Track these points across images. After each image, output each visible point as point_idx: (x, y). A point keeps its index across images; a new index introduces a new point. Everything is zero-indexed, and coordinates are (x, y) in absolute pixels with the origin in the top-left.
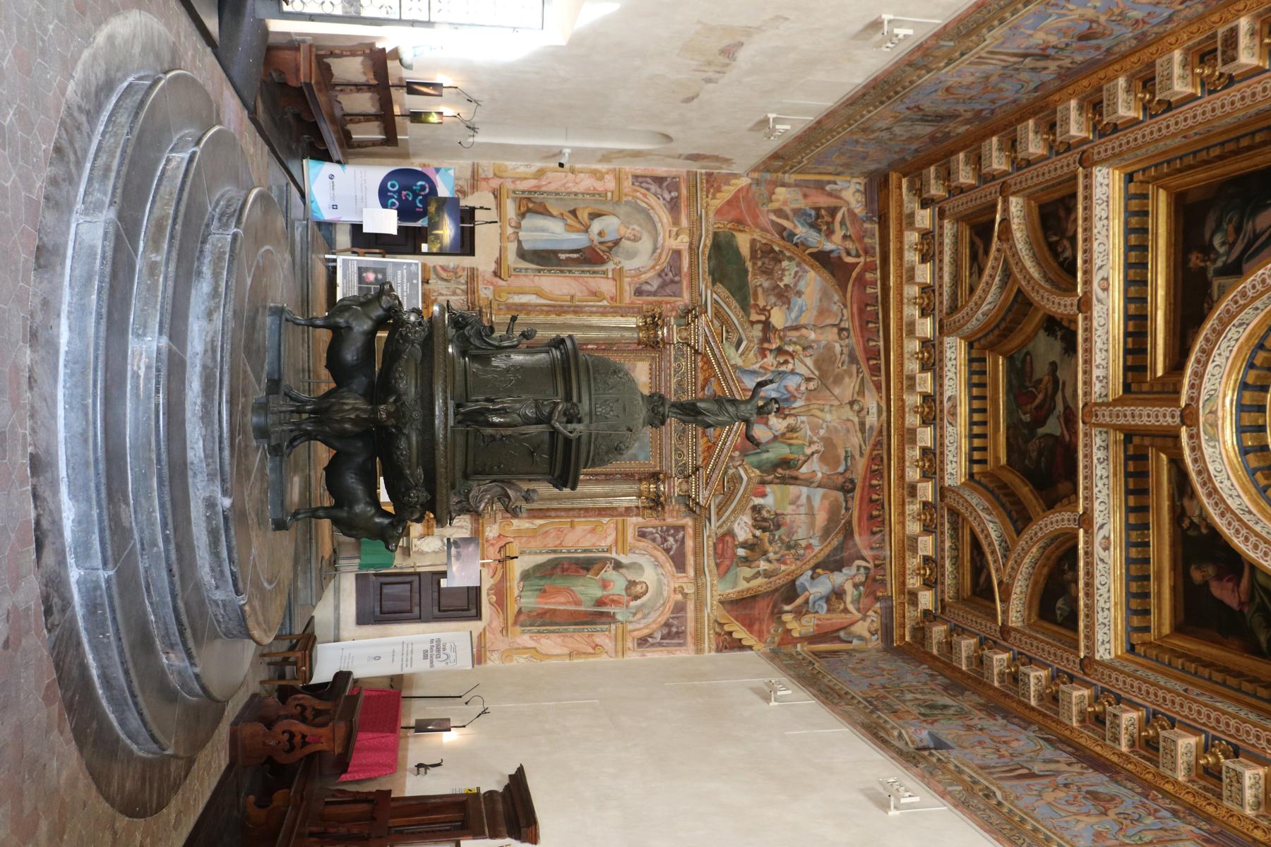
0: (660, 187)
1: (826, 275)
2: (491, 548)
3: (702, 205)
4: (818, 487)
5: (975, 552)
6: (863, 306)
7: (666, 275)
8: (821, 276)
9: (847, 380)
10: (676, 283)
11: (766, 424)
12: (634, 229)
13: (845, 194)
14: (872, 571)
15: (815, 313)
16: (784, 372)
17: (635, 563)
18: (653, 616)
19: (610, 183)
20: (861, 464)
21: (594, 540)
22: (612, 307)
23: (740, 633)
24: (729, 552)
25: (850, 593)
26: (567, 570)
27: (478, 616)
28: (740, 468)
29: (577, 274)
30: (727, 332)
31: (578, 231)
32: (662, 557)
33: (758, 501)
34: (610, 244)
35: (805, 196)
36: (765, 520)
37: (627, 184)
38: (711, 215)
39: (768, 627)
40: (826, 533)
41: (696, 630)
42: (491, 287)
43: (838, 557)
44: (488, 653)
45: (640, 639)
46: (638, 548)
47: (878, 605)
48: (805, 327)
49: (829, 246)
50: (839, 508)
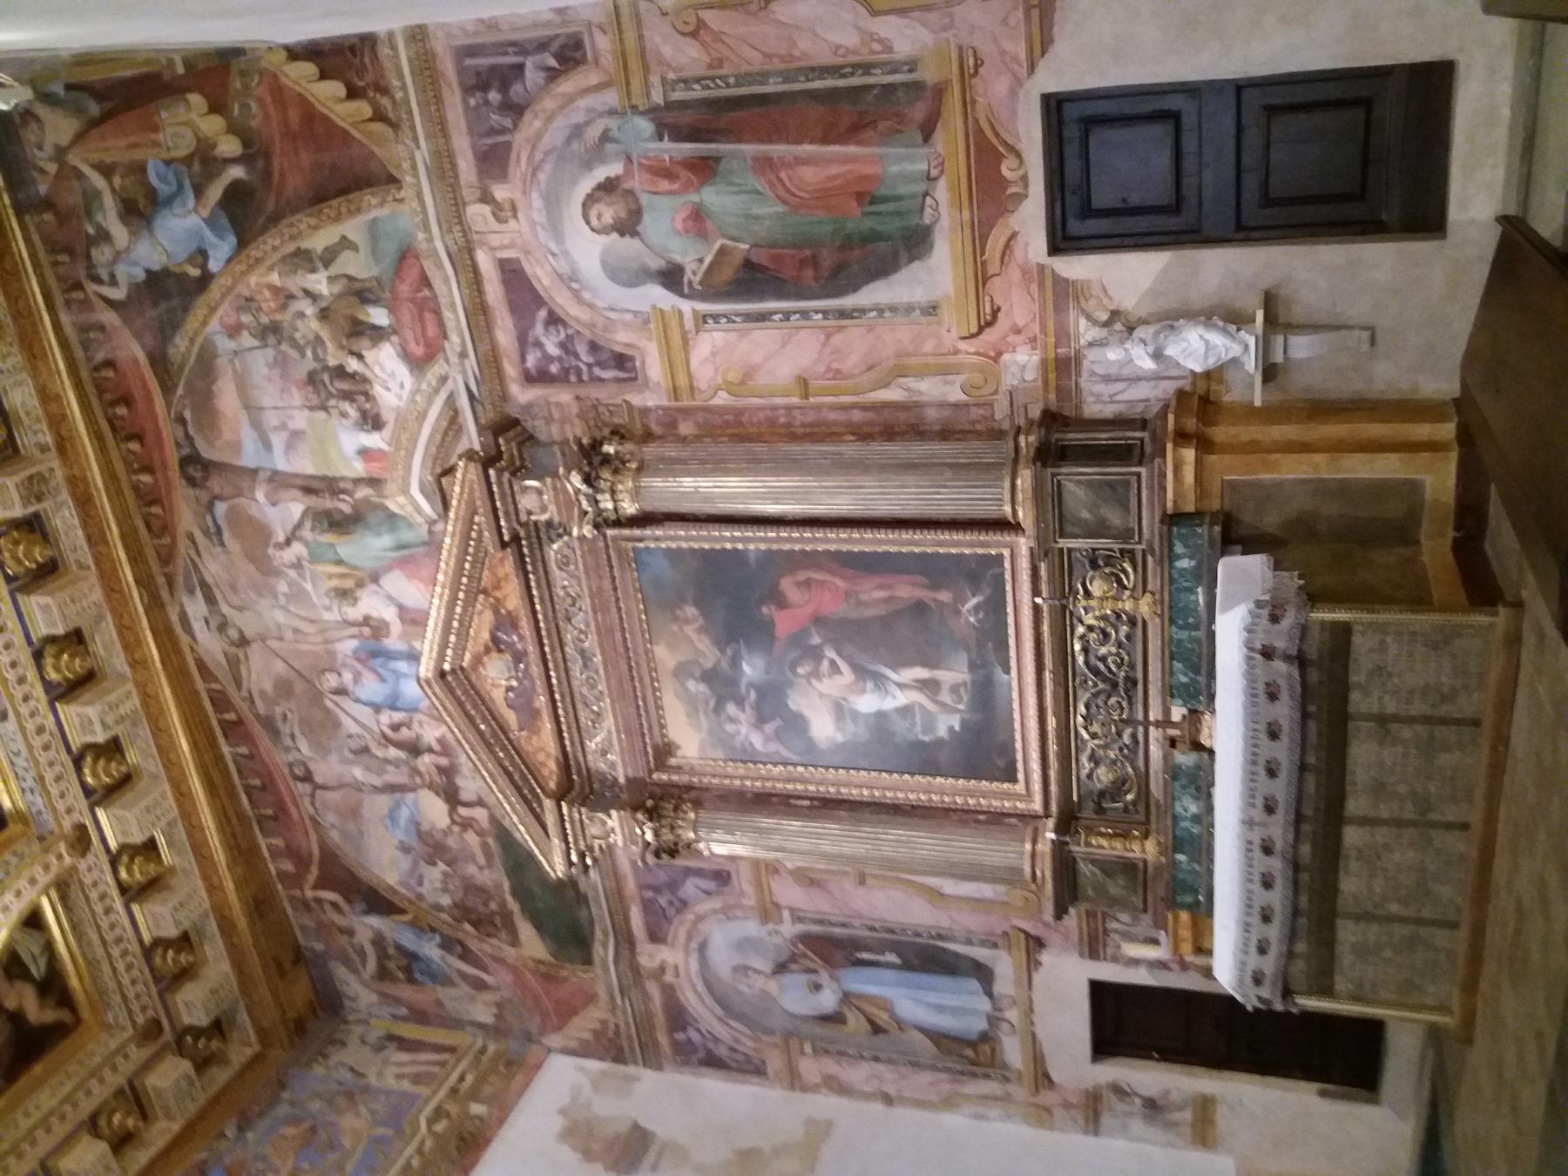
0: (709, 1052)
1: (362, 874)
2: (1020, 322)
3: (625, 1013)
7: (671, 903)
9: (268, 687)
10: (649, 887)
11: (402, 609)
13: (374, 998)
14: (82, 274)
16: (394, 708)
17: (630, 284)
18: (555, 136)
20: (186, 519)
23: (328, 93)
24: (406, 317)
25: (110, 217)
26: (803, 263)
27: (1054, 106)
29: (856, 923)
31: (861, 997)
32: (562, 301)
33: (374, 440)
34: (794, 967)
35: (439, 1004)
36: (348, 396)
37: (775, 1062)
39: (267, 116)
40: (206, 364)
41: (438, 98)
43: (164, 305)
46: (627, 325)
48: (377, 790)
49: (374, 921)
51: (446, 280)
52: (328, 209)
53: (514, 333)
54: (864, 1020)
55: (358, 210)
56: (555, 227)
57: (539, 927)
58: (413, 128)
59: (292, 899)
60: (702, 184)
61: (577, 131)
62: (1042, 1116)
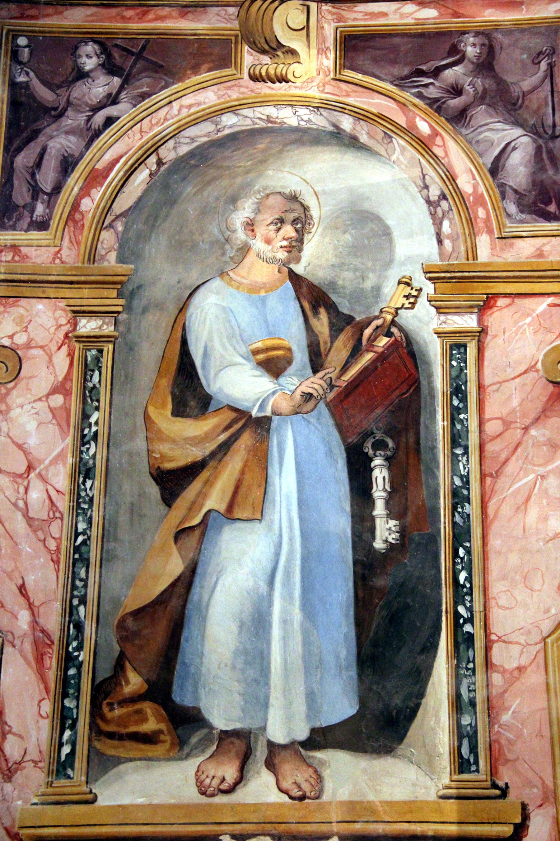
12: (250, 226)
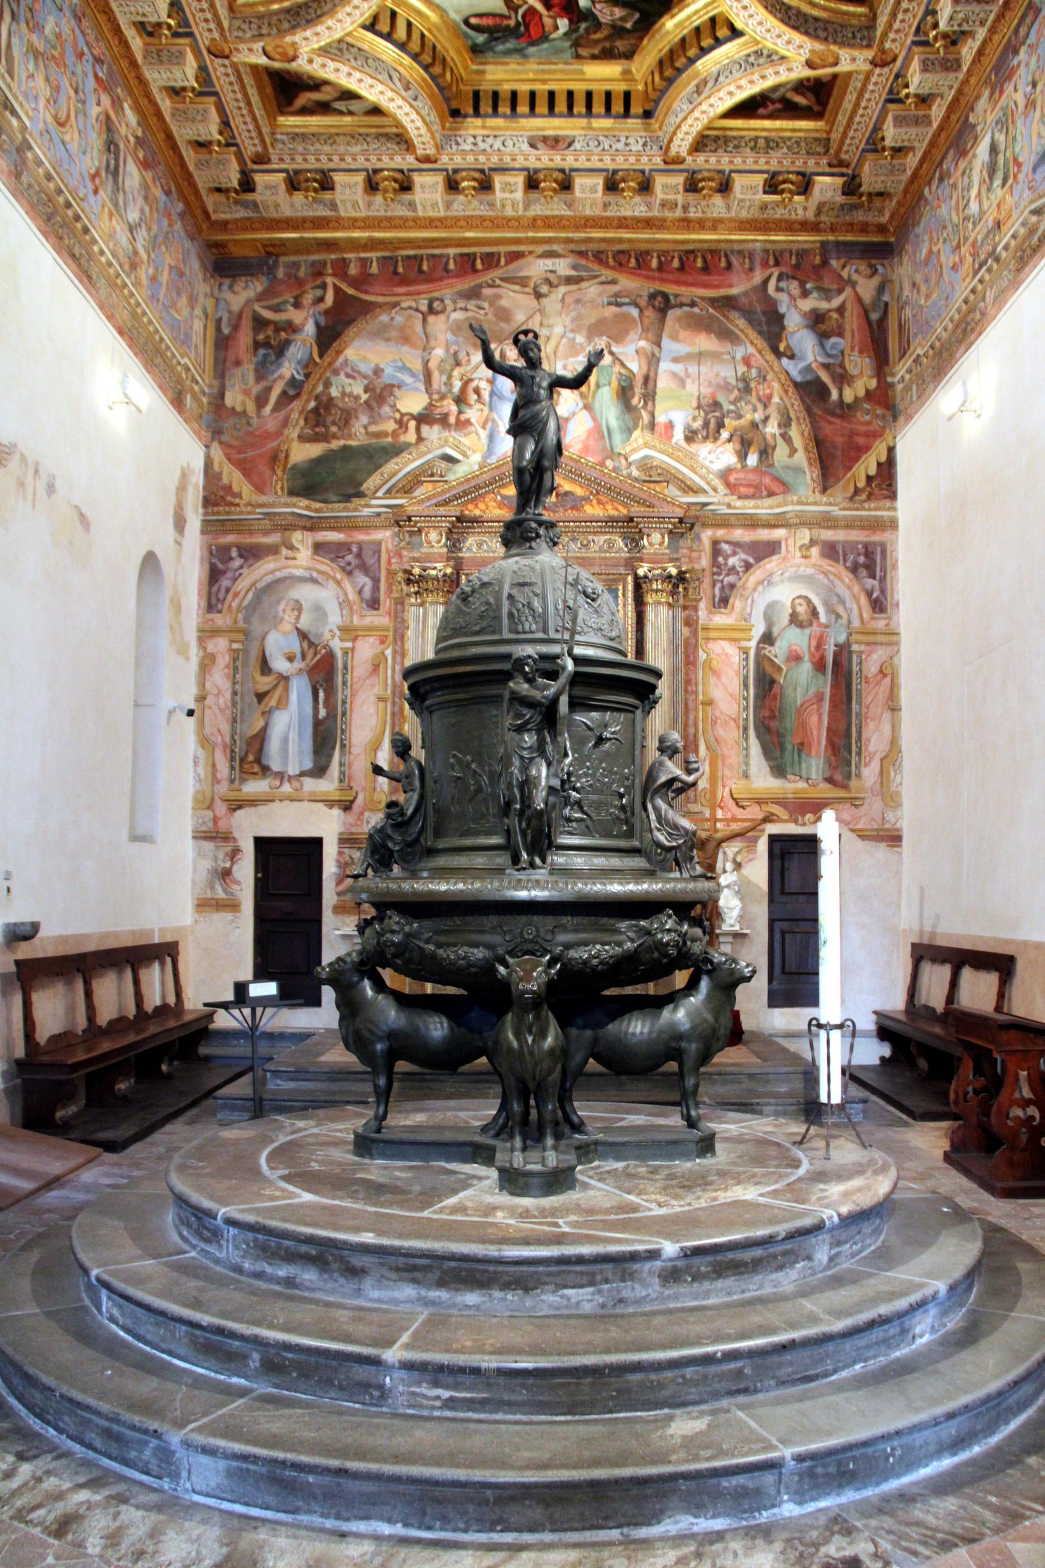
0: (224, 573)
1: (351, 331)
3: (249, 513)
4: (659, 345)
5: (761, 111)
6: (397, 279)
7: (349, 564)
8: (353, 339)
9: (504, 303)
10: (360, 549)
11: (567, 420)
12: (284, 611)
14: (784, 270)
15: (406, 349)
16: (492, 393)
17: (765, 614)
18: (841, 589)
19: (220, 645)
20: (627, 283)
21: (731, 673)
22: (395, 642)
23: (868, 464)
24: (751, 477)
26: (772, 711)
28: (630, 460)
29: (348, 692)
30: (432, 475)
31: (286, 689)
32: (756, 575)
33: (678, 435)
34: (305, 645)
35: (238, 363)
36: (706, 424)
37: (221, 620)
38: (263, 499)
40: (726, 335)
42: (367, 814)
44: (887, 826)
45: (874, 609)
46: (744, 609)
47: (834, 263)
48: (426, 364)
49: (310, 329)
50: (691, 316)
51: (771, 507)
52: (812, 444)
53: (741, 540)
54: (267, 688)
55: (810, 464)
56: (796, 578)
57: (318, 462)
58: (850, 509)
59: (324, 264)
60: (813, 663)
61: (842, 602)
62: (204, 803)
